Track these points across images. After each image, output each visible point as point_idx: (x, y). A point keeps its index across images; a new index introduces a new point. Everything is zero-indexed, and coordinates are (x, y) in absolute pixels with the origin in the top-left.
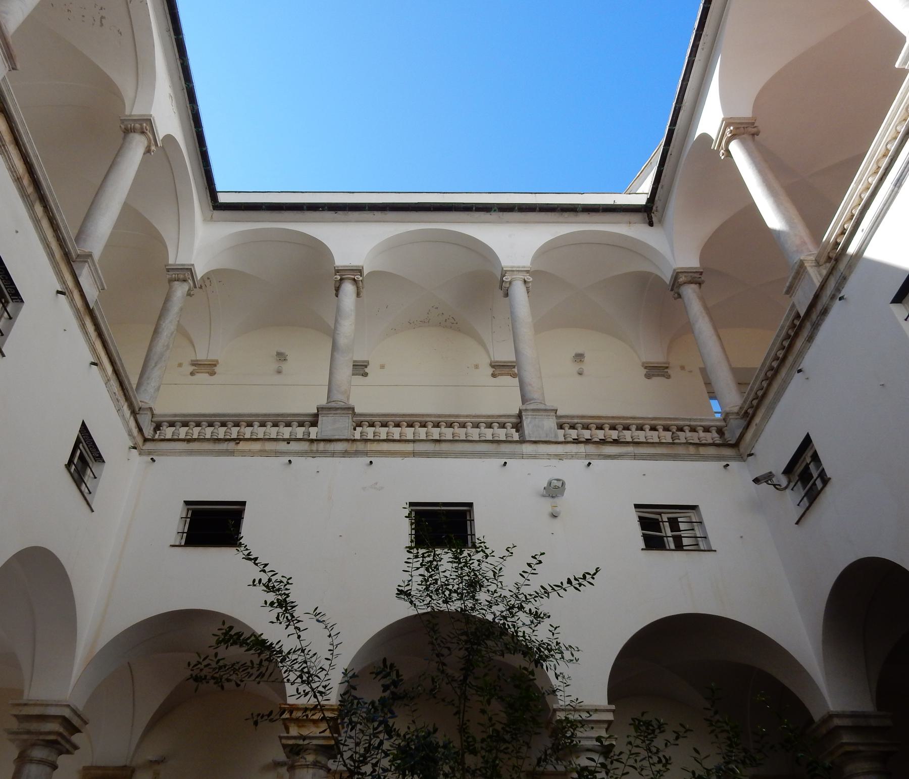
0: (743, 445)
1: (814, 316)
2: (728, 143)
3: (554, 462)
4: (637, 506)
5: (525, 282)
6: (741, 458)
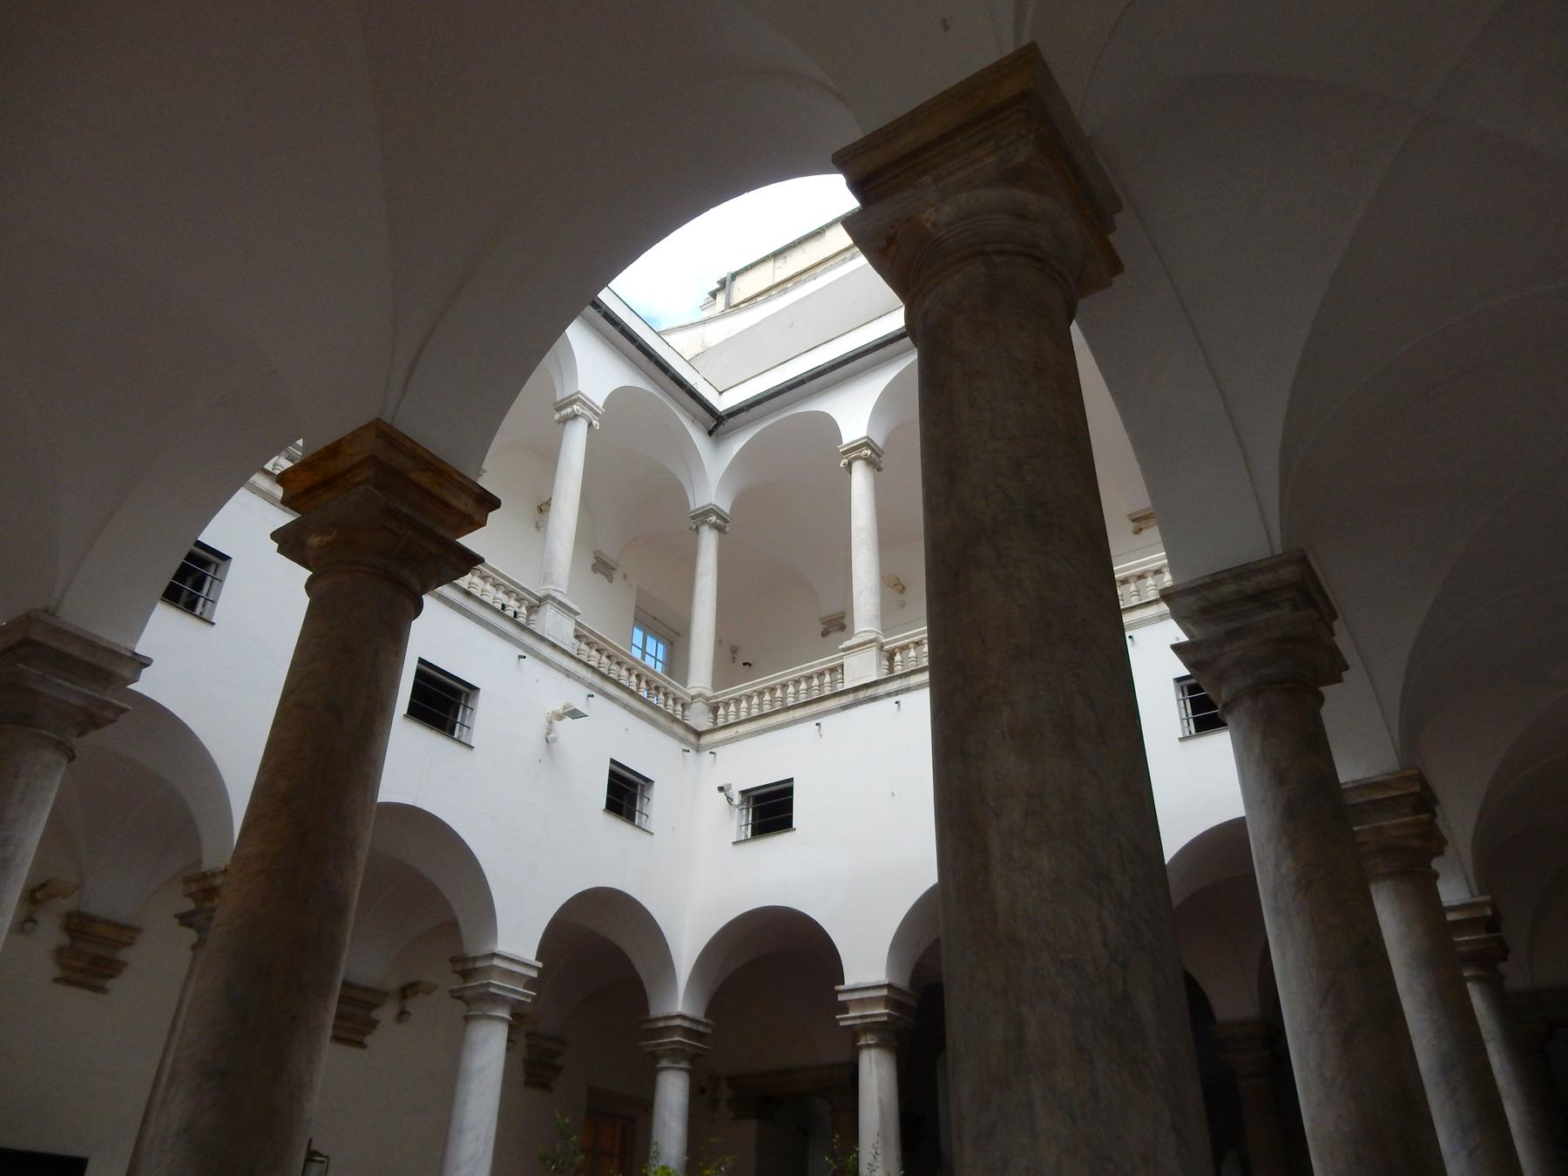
0: (705, 740)
1: (861, 695)
2: (856, 459)
3: (560, 677)
4: (612, 761)
5: (590, 424)
6: (698, 749)
